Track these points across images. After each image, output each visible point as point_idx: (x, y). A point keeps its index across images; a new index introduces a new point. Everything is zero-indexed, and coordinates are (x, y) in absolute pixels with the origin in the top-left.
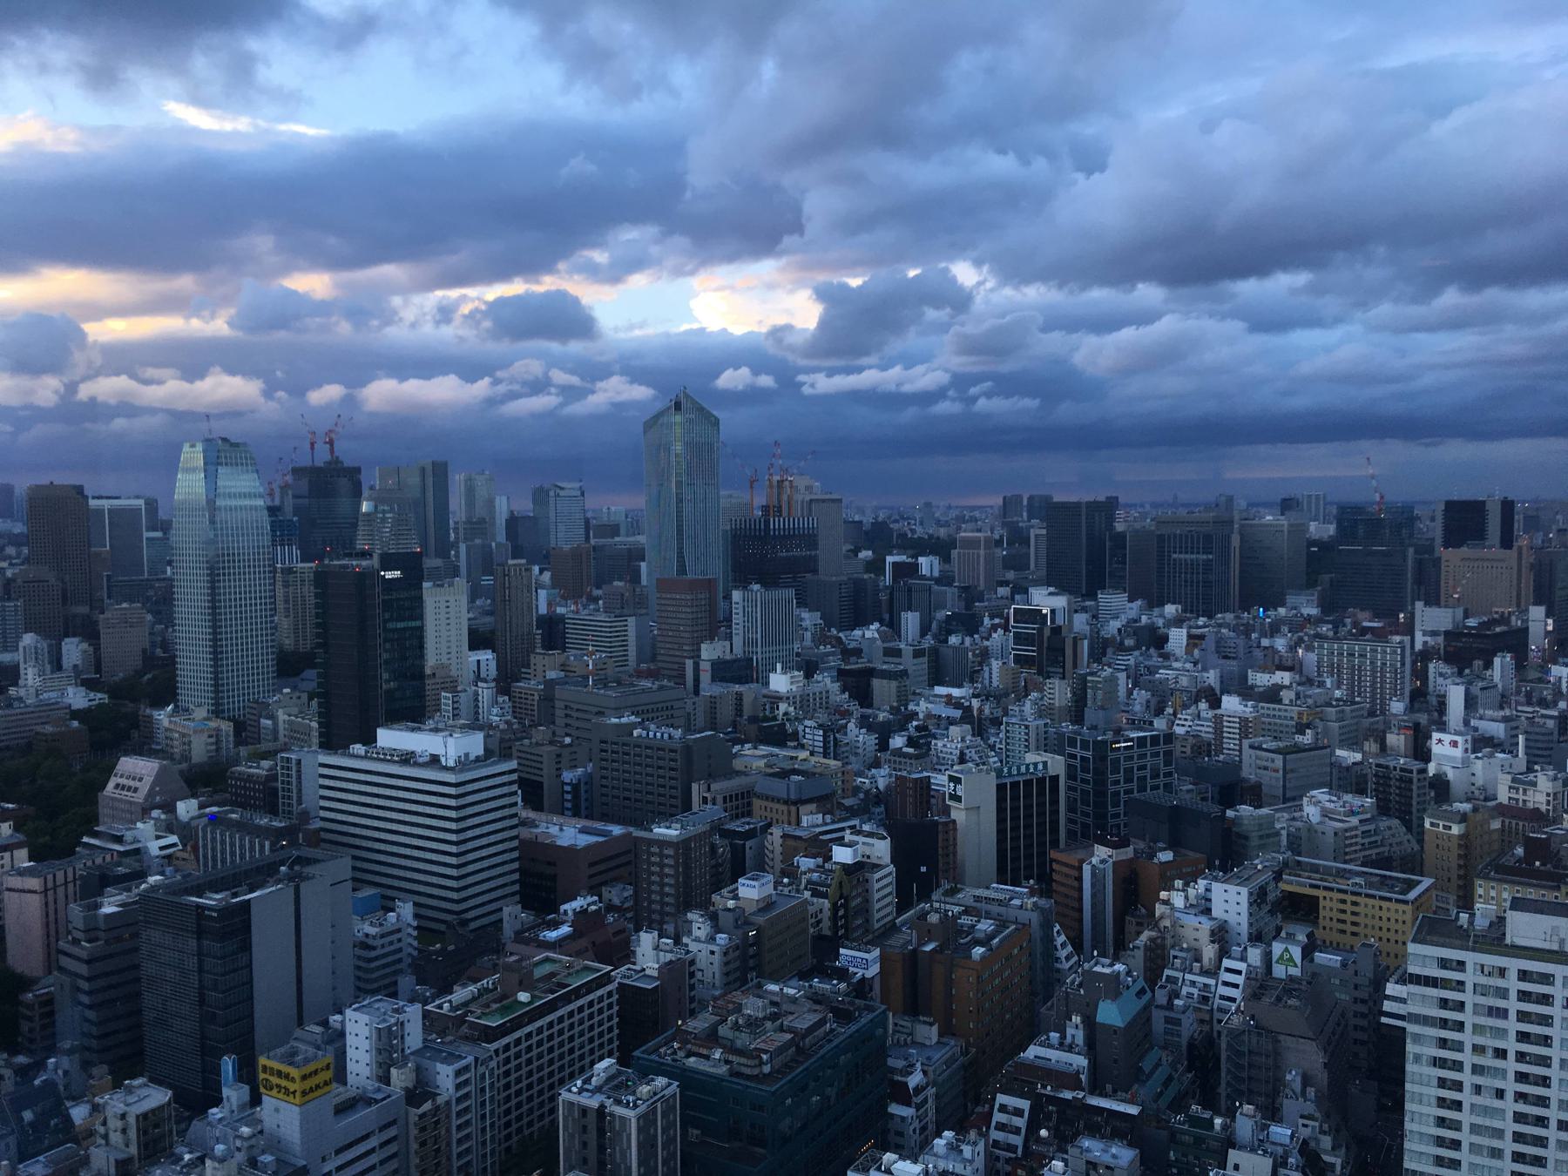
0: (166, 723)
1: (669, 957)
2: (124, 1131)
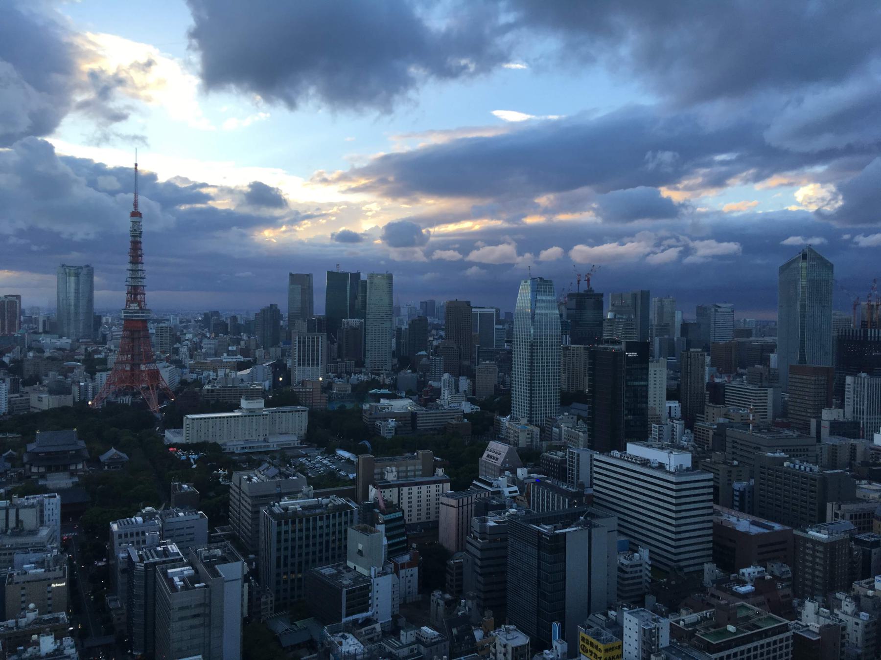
0: (507, 424)
1: (828, 622)
2: (505, 655)
